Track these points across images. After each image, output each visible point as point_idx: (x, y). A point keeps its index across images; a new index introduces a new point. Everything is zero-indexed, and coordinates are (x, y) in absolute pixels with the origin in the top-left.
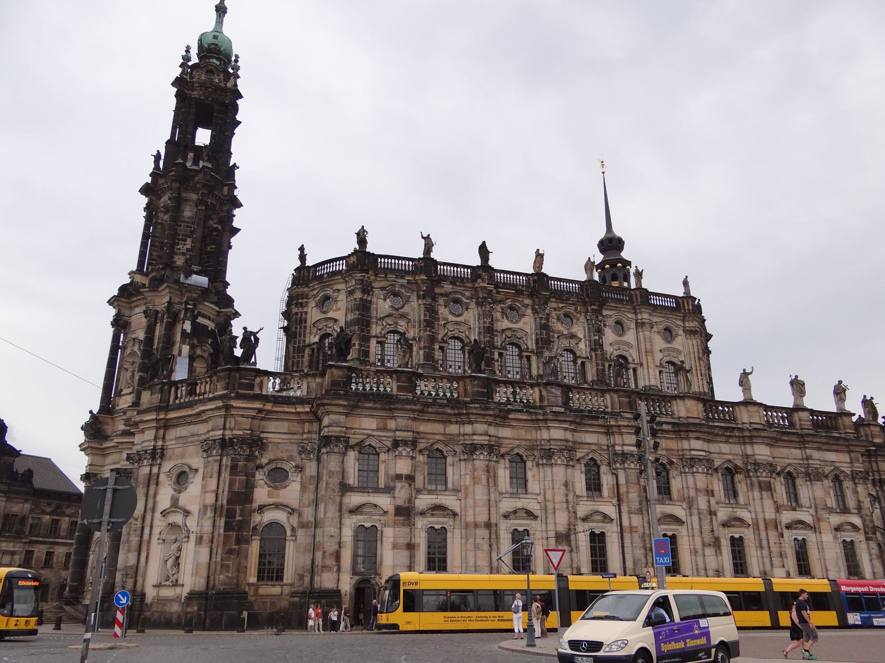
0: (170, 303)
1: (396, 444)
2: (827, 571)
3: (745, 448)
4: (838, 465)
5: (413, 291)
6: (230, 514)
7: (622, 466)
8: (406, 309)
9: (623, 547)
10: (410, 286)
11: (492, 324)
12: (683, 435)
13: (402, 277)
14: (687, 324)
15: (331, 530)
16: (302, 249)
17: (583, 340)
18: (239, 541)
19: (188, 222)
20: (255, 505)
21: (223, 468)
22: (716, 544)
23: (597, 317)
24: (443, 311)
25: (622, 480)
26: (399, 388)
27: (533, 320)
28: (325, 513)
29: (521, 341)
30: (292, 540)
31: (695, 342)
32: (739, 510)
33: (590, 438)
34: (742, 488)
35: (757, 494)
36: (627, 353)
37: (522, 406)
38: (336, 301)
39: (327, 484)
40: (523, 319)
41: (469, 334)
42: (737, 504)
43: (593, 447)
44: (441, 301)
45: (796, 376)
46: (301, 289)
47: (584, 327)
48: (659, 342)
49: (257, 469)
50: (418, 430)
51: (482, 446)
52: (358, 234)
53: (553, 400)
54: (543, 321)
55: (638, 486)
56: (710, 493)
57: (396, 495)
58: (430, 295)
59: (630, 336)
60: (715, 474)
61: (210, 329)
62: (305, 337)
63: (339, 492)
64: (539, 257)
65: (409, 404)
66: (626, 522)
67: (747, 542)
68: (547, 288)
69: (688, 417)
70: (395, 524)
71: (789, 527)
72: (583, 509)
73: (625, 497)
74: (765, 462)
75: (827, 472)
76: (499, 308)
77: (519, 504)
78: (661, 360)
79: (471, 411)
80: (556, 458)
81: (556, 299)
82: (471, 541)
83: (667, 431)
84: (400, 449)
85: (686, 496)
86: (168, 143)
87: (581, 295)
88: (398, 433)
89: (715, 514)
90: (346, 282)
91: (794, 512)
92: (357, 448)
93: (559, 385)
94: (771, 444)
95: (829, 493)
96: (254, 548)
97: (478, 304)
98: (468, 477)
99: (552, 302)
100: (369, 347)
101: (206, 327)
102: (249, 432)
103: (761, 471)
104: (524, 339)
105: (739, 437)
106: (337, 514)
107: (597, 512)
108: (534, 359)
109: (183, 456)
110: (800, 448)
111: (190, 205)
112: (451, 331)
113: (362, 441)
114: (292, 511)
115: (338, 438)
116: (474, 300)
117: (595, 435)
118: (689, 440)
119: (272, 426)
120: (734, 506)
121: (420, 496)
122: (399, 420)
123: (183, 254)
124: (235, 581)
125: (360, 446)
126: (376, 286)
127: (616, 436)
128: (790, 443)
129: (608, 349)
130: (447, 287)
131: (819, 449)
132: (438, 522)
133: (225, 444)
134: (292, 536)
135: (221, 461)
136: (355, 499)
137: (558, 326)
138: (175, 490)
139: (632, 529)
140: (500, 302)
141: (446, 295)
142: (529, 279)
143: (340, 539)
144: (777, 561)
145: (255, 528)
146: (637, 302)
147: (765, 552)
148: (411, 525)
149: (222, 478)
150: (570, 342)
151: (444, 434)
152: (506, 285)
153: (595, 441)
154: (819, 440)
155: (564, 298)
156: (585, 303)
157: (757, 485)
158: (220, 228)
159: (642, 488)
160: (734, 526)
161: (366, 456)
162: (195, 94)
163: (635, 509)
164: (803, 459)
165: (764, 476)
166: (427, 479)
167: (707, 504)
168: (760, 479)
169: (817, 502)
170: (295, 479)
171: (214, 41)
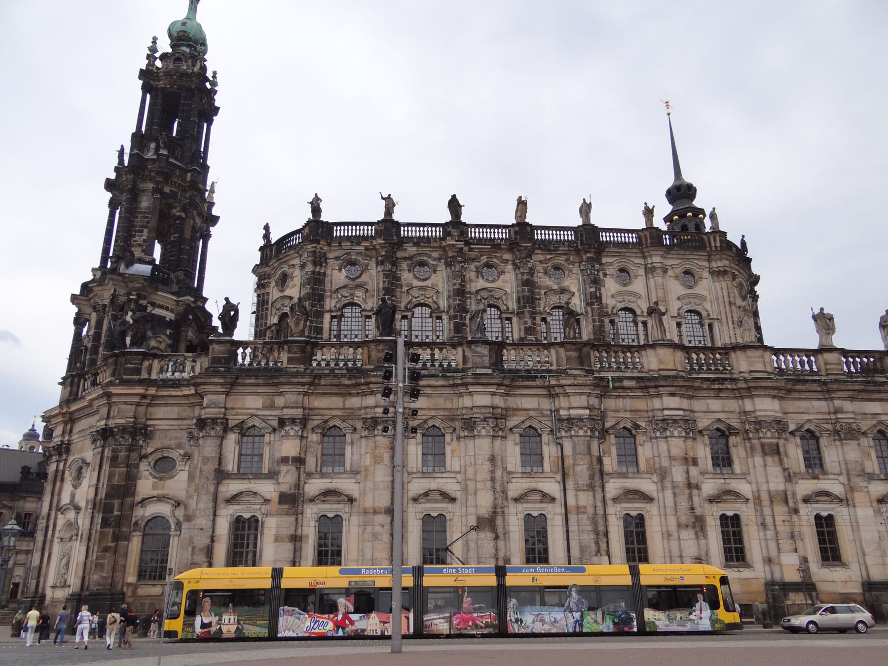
0: (114, 297)
1: (282, 422)
2: (864, 555)
3: (743, 403)
4: (883, 417)
5: (371, 258)
6: (107, 509)
7: (569, 434)
8: (364, 278)
9: (567, 532)
10: (368, 253)
11: (464, 286)
12: (652, 391)
13: (358, 244)
14: (714, 264)
15: (203, 522)
16: (267, 228)
17: (577, 294)
18: (116, 538)
19: (145, 213)
20: (138, 498)
21: (105, 460)
22: (698, 524)
23: (593, 266)
24: (407, 277)
25: (568, 450)
26: (290, 360)
27: (513, 277)
28: (197, 504)
29: (499, 301)
30: (176, 535)
31: (724, 284)
32: (733, 481)
33: (529, 403)
34: (738, 453)
35: (758, 460)
36: (634, 304)
37: (440, 371)
38: (292, 278)
39: (201, 471)
40: (502, 277)
41: (437, 298)
42: (732, 473)
43: (532, 413)
44: (404, 265)
45: (822, 309)
46: (263, 270)
47: (578, 279)
48: (676, 288)
49: (140, 460)
50: (311, 406)
52: (312, 203)
53: (478, 360)
54: (525, 277)
55: (588, 457)
56: (690, 461)
57: (281, 480)
59: (638, 285)
60: (699, 438)
61: (168, 319)
62: (266, 319)
63: (214, 479)
64: (522, 204)
65: (296, 377)
66: (571, 502)
67: (744, 520)
68: (531, 238)
69: (660, 370)
70: (278, 514)
71: (806, 500)
72: (516, 488)
73: (571, 471)
74: (770, 420)
75: (864, 429)
77: (433, 484)
78: (679, 309)
79: (369, 380)
80: (479, 428)
81: (542, 250)
82: (369, 529)
83: (631, 389)
84: (287, 428)
85: (657, 466)
86: (134, 135)
87: (574, 242)
88: (286, 411)
89: (698, 487)
90: (301, 256)
91: (816, 481)
92: (237, 430)
93: (486, 342)
94: (782, 397)
95: (869, 455)
96: (135, 544)
97: (448, 265)
98: (368, 456)
99: (537, 254)
100: (322, 323)
101: (163, 318)
102: (132, 420)
103: (765, 431)
104: (504, 299)
105: (733, 390)
106: (211, 504)
108: (515, 320)
109: (81, 450)
110: (825, 399)
111: (148, 196)
112: (416, 298)
113: (243, 422)
114: (178, 504)
115: (214, 421)
116: (443, 261)
117: (536, 399)
118: (661, 397)
119: (159, 412)
120: (726, 476)
121: (311, 481)
122: (288, 396)
123: (140, 245)
124: (109, 581)
125: (243, 430)
126: (330, 257)
127: (562, 398)
128: (809, 394)
129: (608, 301)
130: (411, 250)
131: (852, 399)
132: (330, 509)
133: (105, 434)
134: (175, 530)
135: (103, 452)
136: (232, 487)
137: (545, 281)
138: (73, 486)
139: (579, 510)
140: (473, 260)
141: (410, 258)
142: (509, 231)
143: (213, 532)
144: (786, 544)
145: (136, 523)
146: (646, 244)
147: (770, 534)
148: (298, 514)
149: (103, 471)
150: (560, 298)
151: (344, 409)
152: (480, 241)
153: (535, 406)
154: (850, 387)
155: (552, 248)
156: (578, 252)
157: (759, 449)
158: (183, 215)
159: (594, 459)
160: (725, 501)
161: (250, 439)
162: (161, 84)
163: (583, 485)
164: (829, 413)
165: (769, 436)
166: (319, 460)
167: (685, 475)
168: (763, 440)
169: (850, 466)
170: (183, 468)
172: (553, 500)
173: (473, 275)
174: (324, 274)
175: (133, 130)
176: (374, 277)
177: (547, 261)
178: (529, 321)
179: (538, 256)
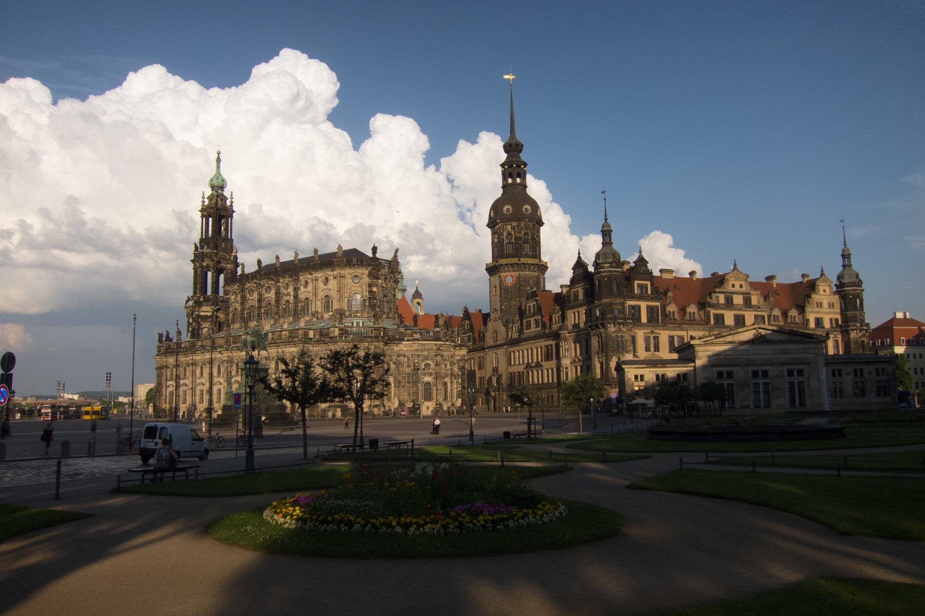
14: (335, 273)
24: (248, 295)
44: (247, 291)
51: (190, 364)
58: (243, 291)
59: (310, 287)
76: (264, 288)
107: (219, 382)
137: (283, 291)
162: (205, 213)
172: (221, 384)
173: (264, 291)
175: (200, 237)
176: (239, 298)
177: (284, 281)
178: (276, 309)
179: (281, 280)
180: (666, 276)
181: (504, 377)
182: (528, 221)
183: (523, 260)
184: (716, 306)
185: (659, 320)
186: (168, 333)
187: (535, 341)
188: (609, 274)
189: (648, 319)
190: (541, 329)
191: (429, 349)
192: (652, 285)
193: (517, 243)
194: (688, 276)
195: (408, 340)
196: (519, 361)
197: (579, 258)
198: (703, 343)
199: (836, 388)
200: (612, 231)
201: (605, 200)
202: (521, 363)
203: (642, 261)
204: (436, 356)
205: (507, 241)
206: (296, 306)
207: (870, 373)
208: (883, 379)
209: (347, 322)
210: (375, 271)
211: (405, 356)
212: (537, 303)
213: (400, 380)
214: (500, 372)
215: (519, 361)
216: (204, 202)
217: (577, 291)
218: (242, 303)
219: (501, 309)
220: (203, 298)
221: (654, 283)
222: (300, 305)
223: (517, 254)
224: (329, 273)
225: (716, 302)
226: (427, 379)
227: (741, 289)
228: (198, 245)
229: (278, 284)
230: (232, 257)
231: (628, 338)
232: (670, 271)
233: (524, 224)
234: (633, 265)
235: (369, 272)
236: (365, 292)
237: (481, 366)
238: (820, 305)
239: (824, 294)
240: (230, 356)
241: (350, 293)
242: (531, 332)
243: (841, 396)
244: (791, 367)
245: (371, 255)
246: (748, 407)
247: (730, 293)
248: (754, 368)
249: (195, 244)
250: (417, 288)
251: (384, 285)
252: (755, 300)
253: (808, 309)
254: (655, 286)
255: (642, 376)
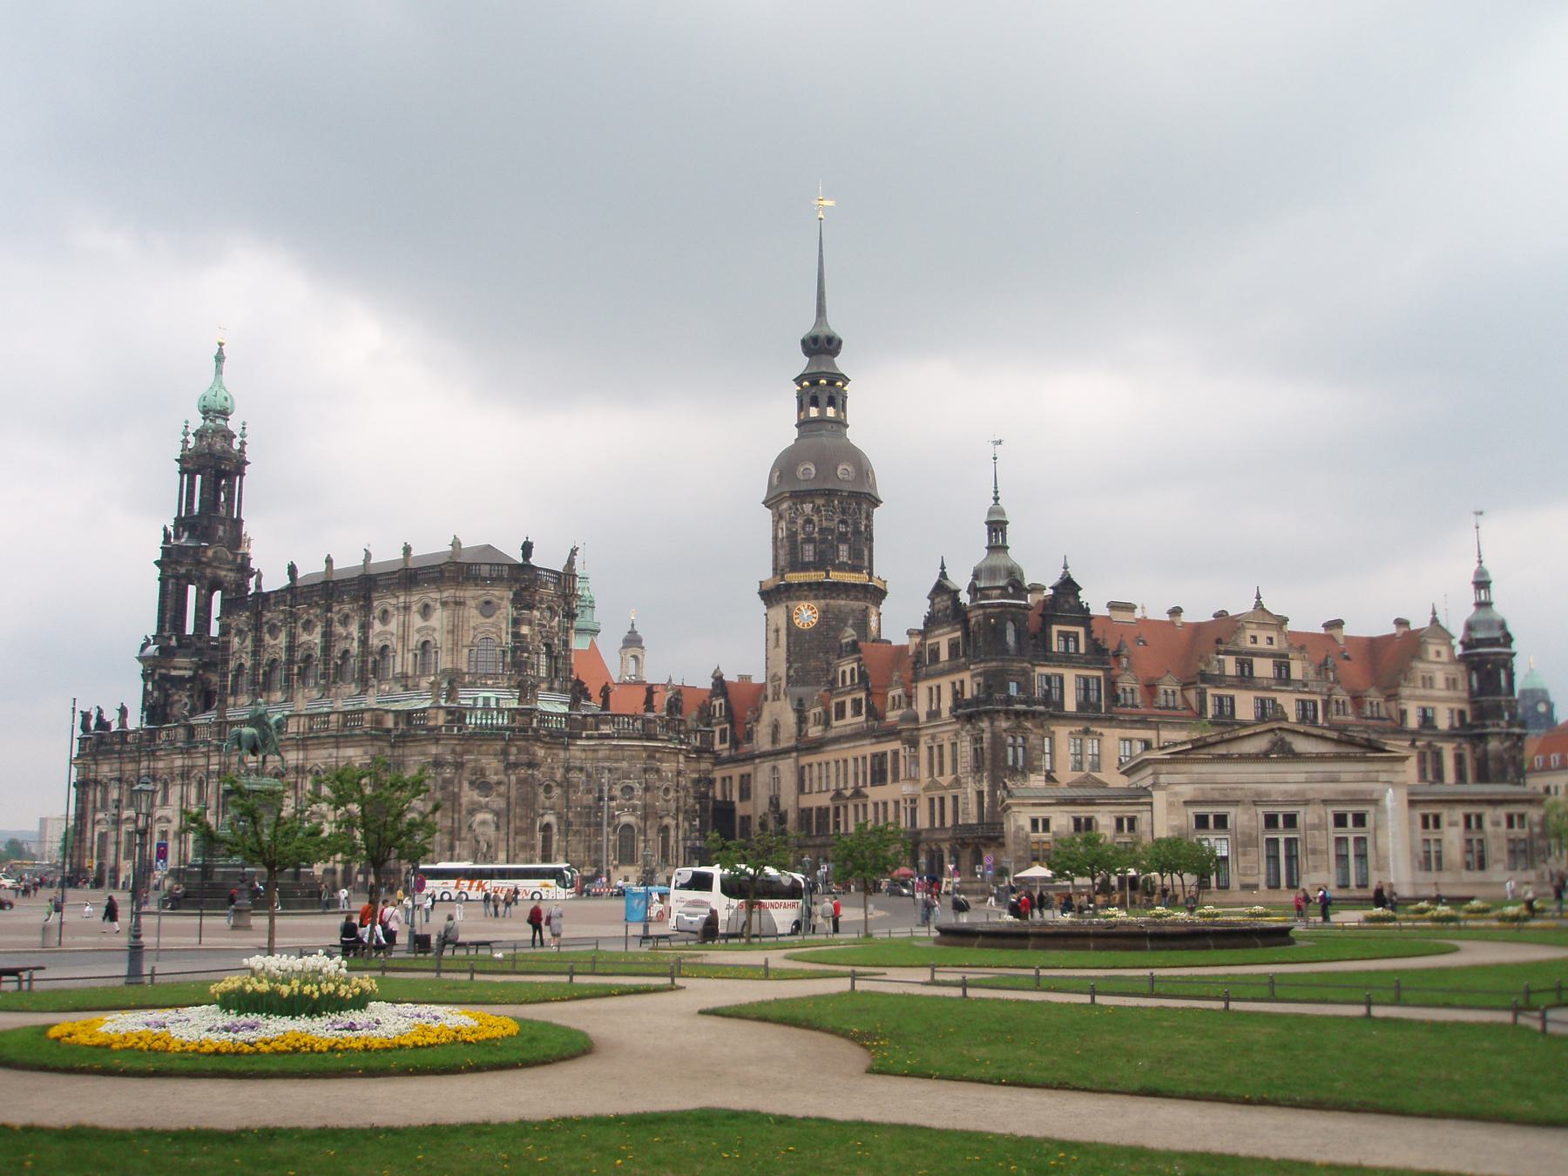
14: (446, 594)
24: (267, 637)
44: (265, 629)
48: (417, 621)
58: (257, 628)
59: (393, 625)
76: (299, 624)
131: (337, 747)
137: (339, 629)
148: (118, 830)
162: (189, 466)
171: (205, 403)
173: (301, 630)
174: (229, 642)
176: (248, 642)
177: (340, 610)
179: (336, 609)
180: (1120, 616)
181: (792, 817)
182: (848, 496)
183: (836, 576)
184: (1219, 680)
185: (1100, 707)
186: (100, 711)
187: (852, 744)
188: (997, 610)
189: (1080, 706)
190: (867, 720)
191: (632, 756)
192: (1089, 633)
193: (824, 541)
194: (1167, 618)
195: (589, 738)
196: (820, 786)
197: (943, 575)
198: (1168, 757)
199: (1429, 852)
200: (1007, 523)
201: (995, 459)
202: (824, 789)
203: (1068, 587)
204: (645, 771)
205: (803, 536)
206: (363, 661)
207: (1496, 824)
208: (1523, 836)
209: (465, 698)
210: (526, 593)
211: (581, 769)
212: (859, 667)
213: (571, 819)
214: (783, 807)
215: (820, 786)
216: (186, 442)
217: (938, 643)
218: (255, 653)
219: (788, 677)
220: (177, 640)
221: (1092, 632)
222: (370, 659)
223: (823, 561)
224: (431, 595)
225: (1217, 673)
226: (626, 819)
227: (1270, 647)
228: (171, 529)
229: (329, 615)
230: (239, 557)
231: (1036, 742)
232: (1130, 608)
233: (839, 502)
234: (1051, 592)
235: (515, 594)
236: (504, 636)
237: (745, 794)
238: (1428, 682)
239: (1438, 660)
240: (225, 763)
241: (475, 637)
242: (845, 726)
243: (1439, 868)
244: (1340, 809)
245: (520, 560)
246: (1256, 887)
247: (1247, 654)
248: (1270, 810)
249: (165, 529)
250: (633, 625)
251: (544, 622)
252: (1297, 670)
253: (1405, 691)
254: (1094, 636)
255: (1046, 822)
